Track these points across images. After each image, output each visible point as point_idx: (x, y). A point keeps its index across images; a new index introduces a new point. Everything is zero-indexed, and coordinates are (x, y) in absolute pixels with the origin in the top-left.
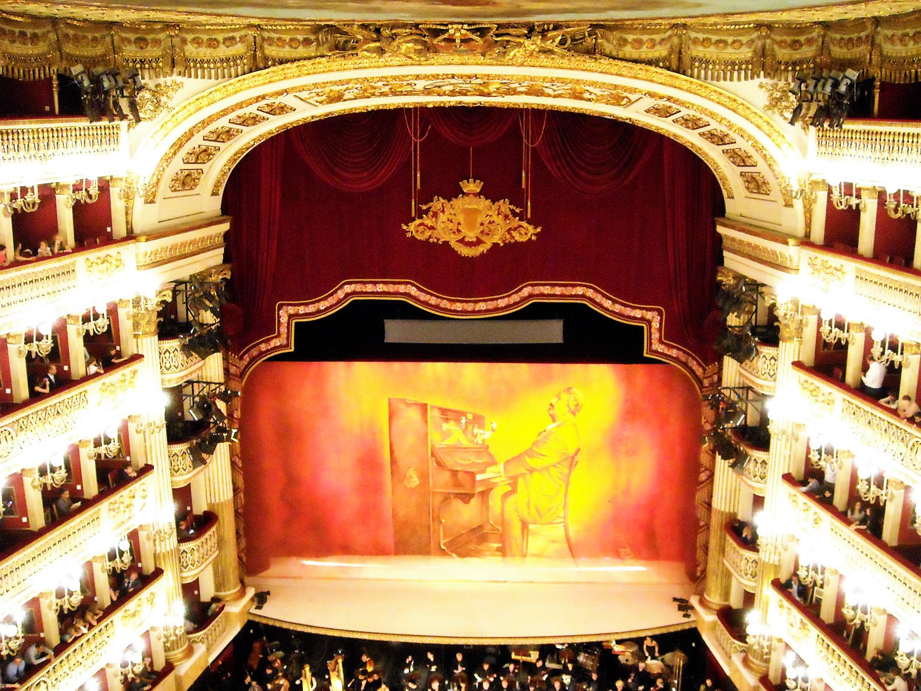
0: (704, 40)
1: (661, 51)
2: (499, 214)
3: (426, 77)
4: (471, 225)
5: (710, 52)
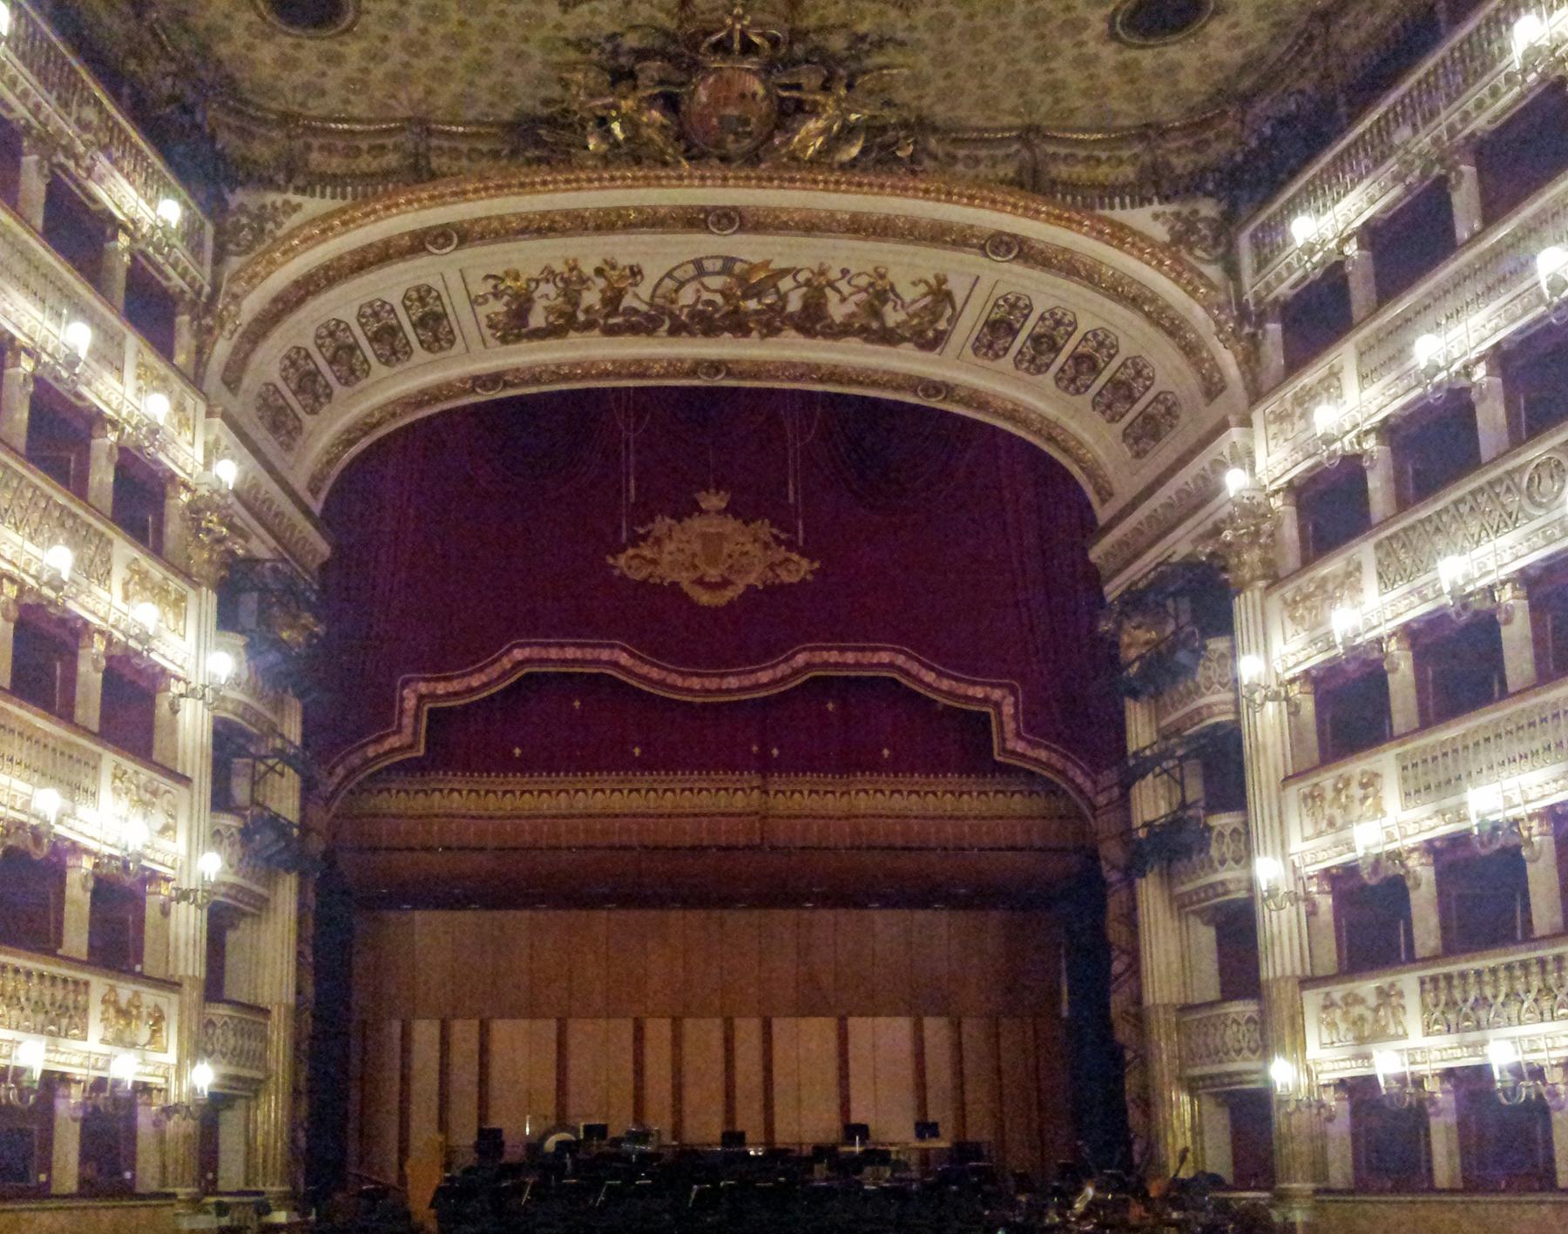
0: (1066, 157)
2: (755, 541)
4: (713, 561)
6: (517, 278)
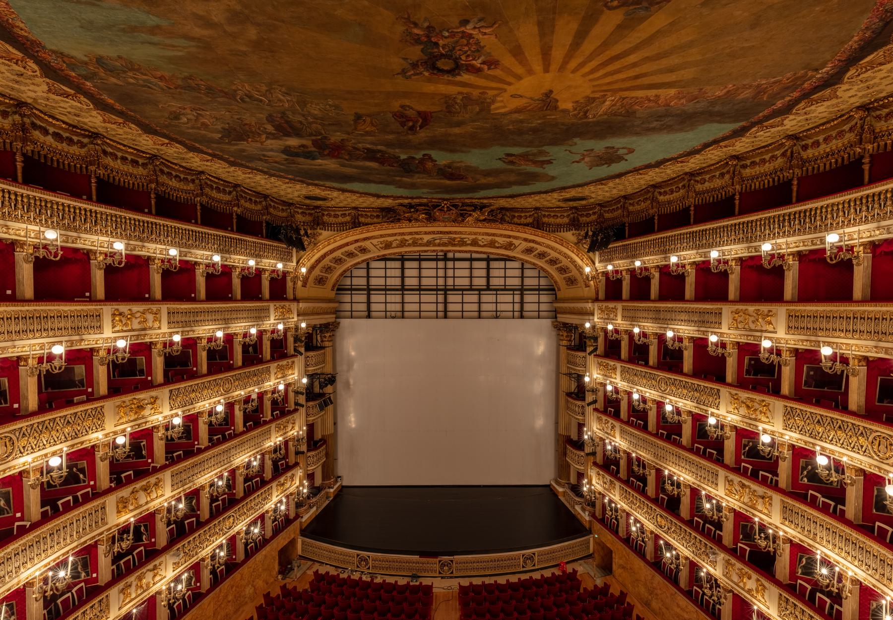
1: (530, 220)
3: (429, 233)
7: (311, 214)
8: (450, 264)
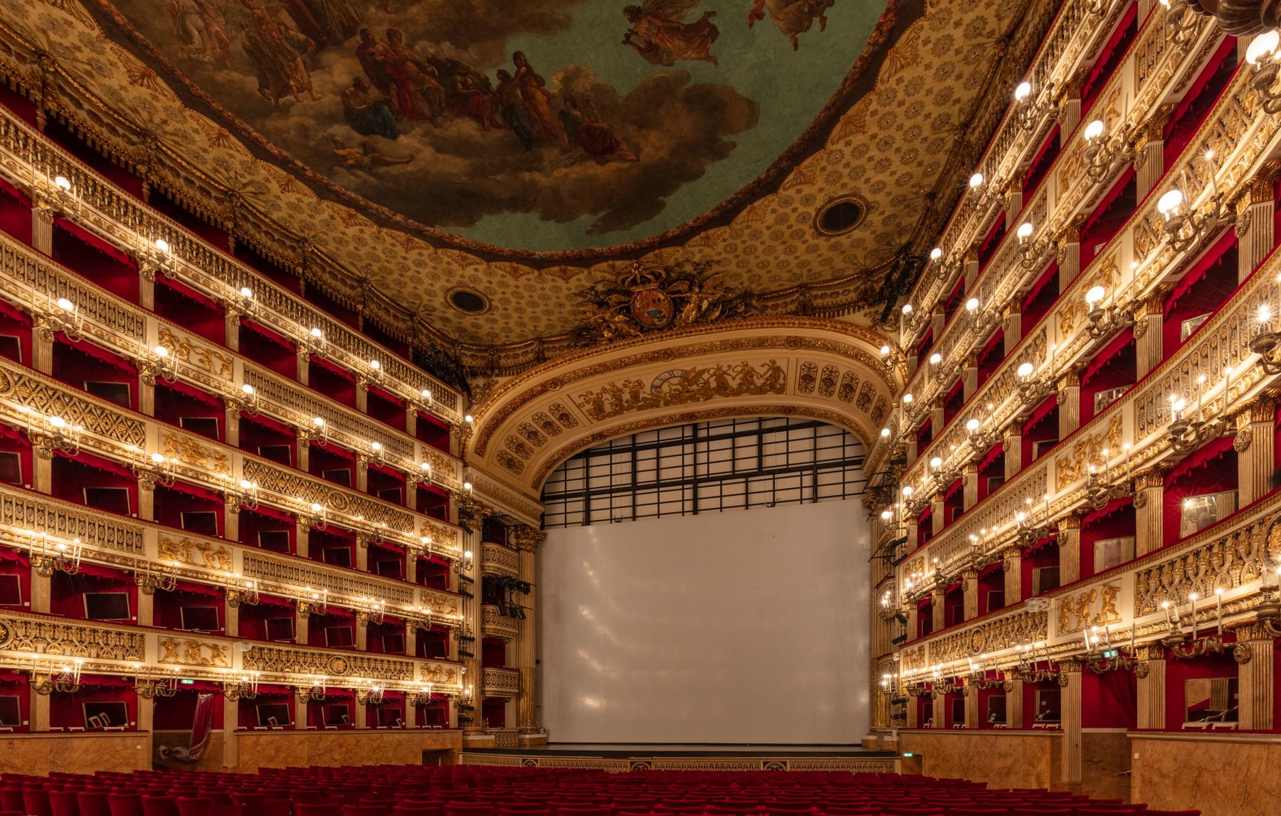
5: (828, 301)
6: (592, 394)
7: (483, 358)
8: (702, 446)
